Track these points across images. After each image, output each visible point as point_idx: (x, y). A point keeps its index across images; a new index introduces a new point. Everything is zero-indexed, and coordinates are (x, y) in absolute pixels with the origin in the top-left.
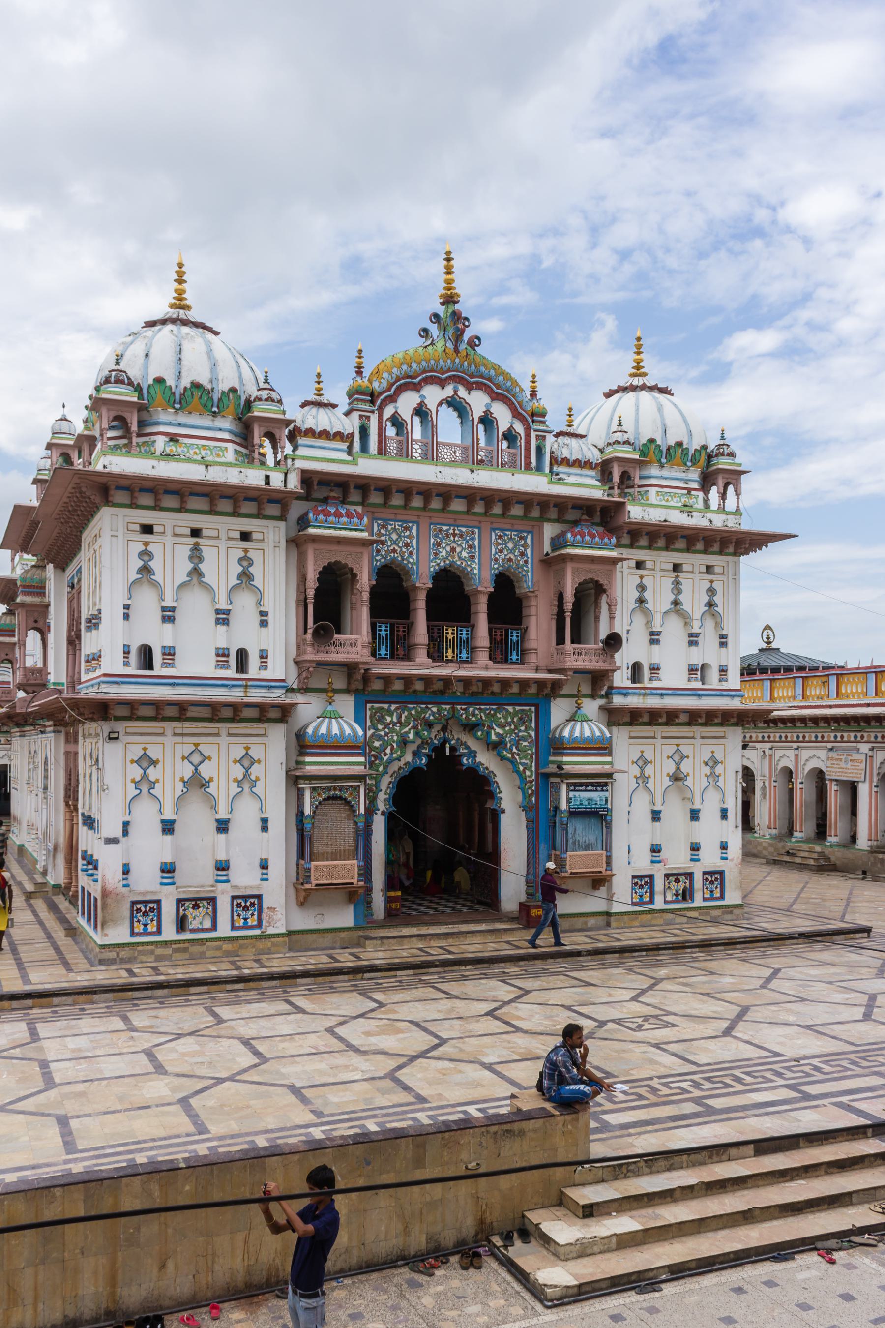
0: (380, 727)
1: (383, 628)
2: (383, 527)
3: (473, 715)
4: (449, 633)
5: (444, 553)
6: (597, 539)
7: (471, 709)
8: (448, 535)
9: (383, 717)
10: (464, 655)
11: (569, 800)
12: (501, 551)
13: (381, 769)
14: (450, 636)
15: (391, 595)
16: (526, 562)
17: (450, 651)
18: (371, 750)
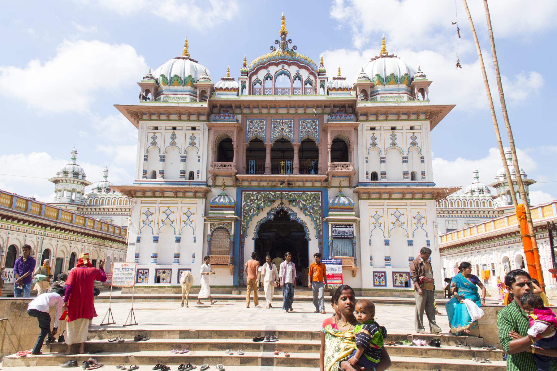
0: (248, 201)
1: (252, 162)
2: (251, 122)
3: (291, 196)
4: (282, 163)
5: (278, 131)
6: (343, 117)
7: (290, 194)
8: (279, 123)
9: (250, 197)
10: (289, 172)
11: (333, 232)
12: (304, 128)
13: (248, 218)
14: (282, 164)
15: (255, 148)
16: (316, 132)
17: (282, 170)
18: (244, 210)
